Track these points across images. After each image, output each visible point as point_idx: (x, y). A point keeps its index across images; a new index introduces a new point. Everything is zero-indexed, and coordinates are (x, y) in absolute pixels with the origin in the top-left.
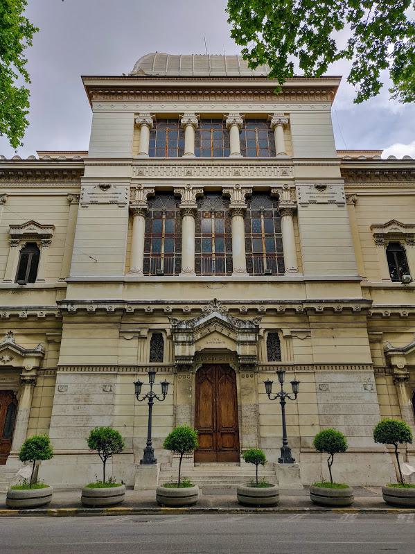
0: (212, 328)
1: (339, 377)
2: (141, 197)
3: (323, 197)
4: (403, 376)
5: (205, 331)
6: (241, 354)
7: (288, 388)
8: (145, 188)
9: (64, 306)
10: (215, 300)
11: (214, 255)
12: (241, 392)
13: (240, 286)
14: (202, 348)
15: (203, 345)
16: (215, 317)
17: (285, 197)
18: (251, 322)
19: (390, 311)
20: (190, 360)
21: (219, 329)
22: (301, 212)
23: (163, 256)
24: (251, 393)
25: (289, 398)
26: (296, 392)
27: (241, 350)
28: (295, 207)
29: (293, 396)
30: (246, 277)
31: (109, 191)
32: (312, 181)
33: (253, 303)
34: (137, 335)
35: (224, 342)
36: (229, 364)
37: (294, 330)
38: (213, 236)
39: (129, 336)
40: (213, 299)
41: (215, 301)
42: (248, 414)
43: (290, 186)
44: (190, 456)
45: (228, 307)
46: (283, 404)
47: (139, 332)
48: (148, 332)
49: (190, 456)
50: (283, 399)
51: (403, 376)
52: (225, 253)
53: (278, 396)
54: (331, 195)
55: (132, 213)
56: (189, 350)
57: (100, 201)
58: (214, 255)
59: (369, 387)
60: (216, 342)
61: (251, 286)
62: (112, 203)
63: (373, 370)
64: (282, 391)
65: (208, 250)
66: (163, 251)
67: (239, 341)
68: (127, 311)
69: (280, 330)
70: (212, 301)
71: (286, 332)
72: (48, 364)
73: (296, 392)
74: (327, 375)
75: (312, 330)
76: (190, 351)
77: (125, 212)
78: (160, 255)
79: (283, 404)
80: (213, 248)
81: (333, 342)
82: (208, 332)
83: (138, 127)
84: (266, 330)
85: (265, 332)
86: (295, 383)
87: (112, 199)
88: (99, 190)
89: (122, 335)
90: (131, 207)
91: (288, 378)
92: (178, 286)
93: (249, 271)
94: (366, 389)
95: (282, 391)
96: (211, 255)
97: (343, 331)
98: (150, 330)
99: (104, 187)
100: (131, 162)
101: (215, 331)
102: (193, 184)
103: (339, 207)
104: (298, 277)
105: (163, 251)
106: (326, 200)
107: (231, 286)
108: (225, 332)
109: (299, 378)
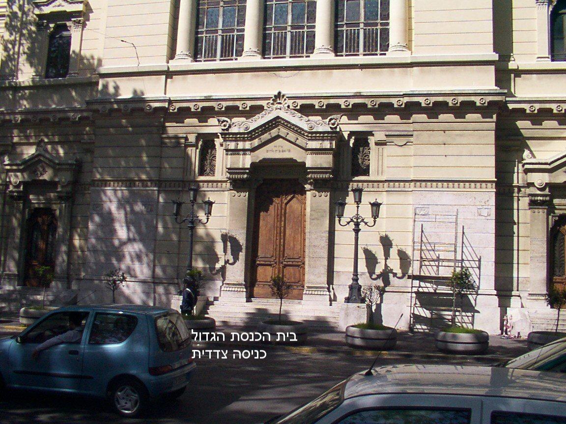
0: (274, 132)
1: (446, 198)
4: (541, 198)
5: (266, 137)
6: (310, 166)
7: (365, 211)
9: (95, 107)
10: (279, 93)
11: (289, 29)
15: (264, 154)
16: (278, 117)
19: (537, 106)
20: (244, 173)
21: (283, 131)
24: (323, 216)
25: (366, 223)
26: (375, 215)
27: (310, 161)
29: (371, 221)
30: (331, 58)
35: (289, 151)
37: (390, 133)
40: (276, 93)
41: (279, 96)
44: (242, 290)
45: (300, 102)
46: (357, 231)
49: (242, 290)
50: (357, 225)
51: (541, 198)
52: (306, 23)
53: (352, 220)
56: (243, 160)
58: (289, 29)
59: (485, 212)
60: (279, 150)
63: (495, 190)
64: (358, 215)
65: (281, 21)
66: (220, 26)
67: (307, 150)
69: (371, 133)
70: (275, 96)
71: (379, 136)
72: (86, 178)
73: (375, 215)
74: (429, 195)
75: (415, 133)
76: (246, 161)
79: (357, 231)
80: (290, 17)
81: (442, 150)
82: (269, 137)
84: (352, 134)
85: (350, 136)
86: (376, 206)
91: (367, 198)
93: (337, 49)
94: (480, 215)
95: (358, 215)
96: (286, 28)
97: (461, 135)
98: (199, 136)
101: (278, 137)
104: (406, 57)
105: (220, 26)
108: (292, 136)
109: (382, 198)
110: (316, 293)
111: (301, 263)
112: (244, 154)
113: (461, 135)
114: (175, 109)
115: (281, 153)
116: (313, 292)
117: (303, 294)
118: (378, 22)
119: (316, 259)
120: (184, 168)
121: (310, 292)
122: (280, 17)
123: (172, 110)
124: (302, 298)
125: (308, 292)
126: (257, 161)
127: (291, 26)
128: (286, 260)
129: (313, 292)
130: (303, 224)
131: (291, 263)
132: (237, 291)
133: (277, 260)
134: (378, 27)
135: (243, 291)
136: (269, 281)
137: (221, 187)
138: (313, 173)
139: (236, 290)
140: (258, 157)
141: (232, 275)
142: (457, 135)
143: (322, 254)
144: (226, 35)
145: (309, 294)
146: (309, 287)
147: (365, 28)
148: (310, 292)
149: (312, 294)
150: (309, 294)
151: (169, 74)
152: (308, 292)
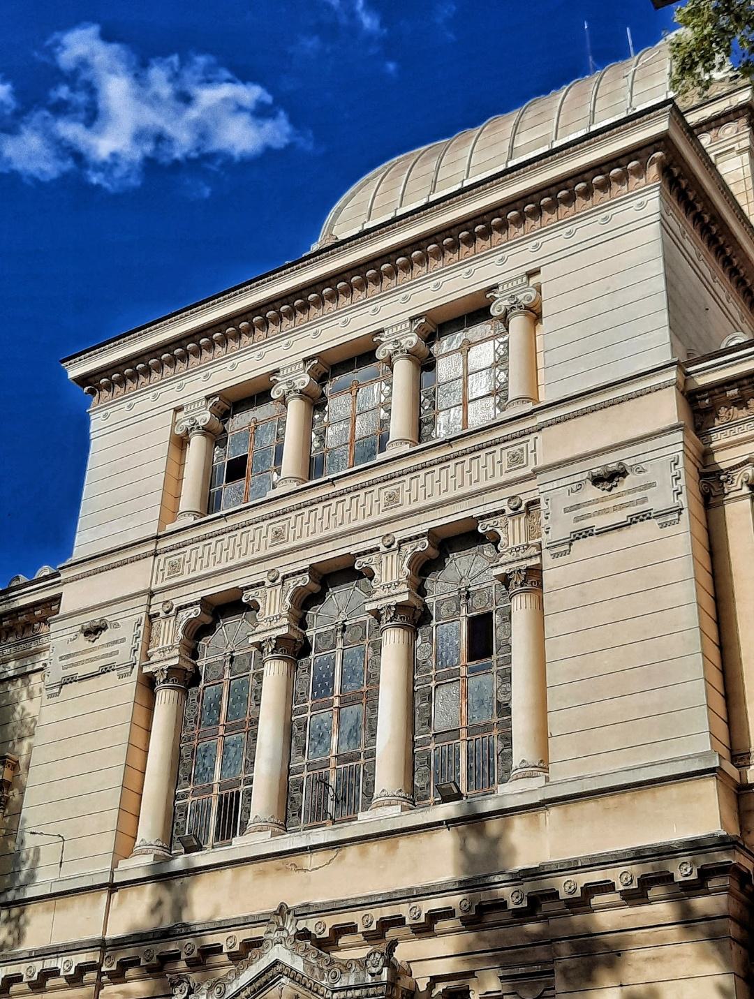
2: (169, 635)
3: (616, 508)
8: (180, 608)
10: (281, 907)
13: (375, 849)
17: (513, 534)
18: (362, 963)
22: (548, 578)
23: (216, 791)
28: (536, 561)
31: (104, 637)
32: (577, 467)
33: (391, 899)
38: (337, 703)
41: (282, 911)
43: (526, 499)
54: (638, 496)
55: (149, 684)
57: (82, 671)
61: (404, 843)
62: (105, 670)
65: (320, 749)
66: (217, 778)
70: (275, 913)
77: (128, 688)
78: (211, 788)
80: (335, 738)
83: (181, 443)
87: (103, 662)
88: (83, 643)
90: (146, 670)
92: (228, 873)
99: (93, 631)
100: (150, 547)
102: (285, 566)
103: (662, 526)
105: (217, 778)
106: (620, 517)
107: (352, 852)
113: (654, 959)
118: (493, 721)
122: (319, 742)
127: (336, 756)
134: (493, 734)
142: (647, 960)
144: (233, 793)
147: (468, 739)
151: (112, 887)
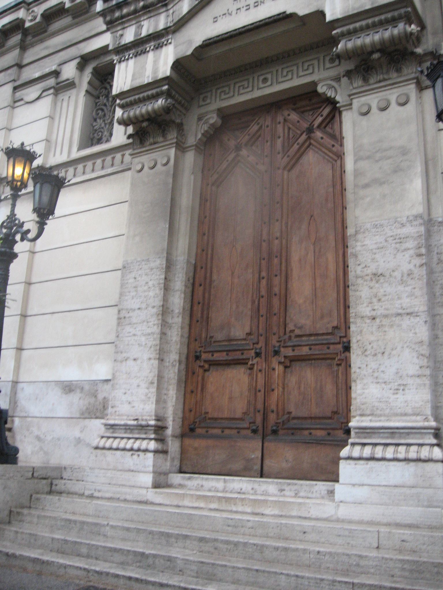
6: (339, 15)
12: (357, 173)
14: (198, 41)
34: (51, 82)
36: (314, 84)
39: (32, 93)
42: (384, 262)
44: (144, 445)
47: (56, 73)
48: (81, 67)
49: (144, 445)
68: (27, 25)
89: (18, 94)
98: (84, 60)
110: (390, 452)
111: (340, 347)
112: (158, 47)
114: (35, 18)
115: (252, 10)
116: (379, 452)
117: (340, 458)
119: (385, 322)
120: (47, 140)
121: (367, 451)
123: (31, 21)
124: (338, 475)
125: (356, 452)
126: (189, 52)
128: (289, 344)
129: (379, 452)
130: (339, 213)
131: (305, 351)
132: (132, 449)
133: (262, 344)
135: (146, 451)
136: (239, 415)
137: (122, 162)
138: (350, 34)
139: (128, 446)
140: (190, 42)
141: (124, 398)
143: (406, 302)
145: (360, 459)
146: (364, 431)
148: (367, 451)
149: (372, 459)
150: (360, 459)
152: (356, 452)
